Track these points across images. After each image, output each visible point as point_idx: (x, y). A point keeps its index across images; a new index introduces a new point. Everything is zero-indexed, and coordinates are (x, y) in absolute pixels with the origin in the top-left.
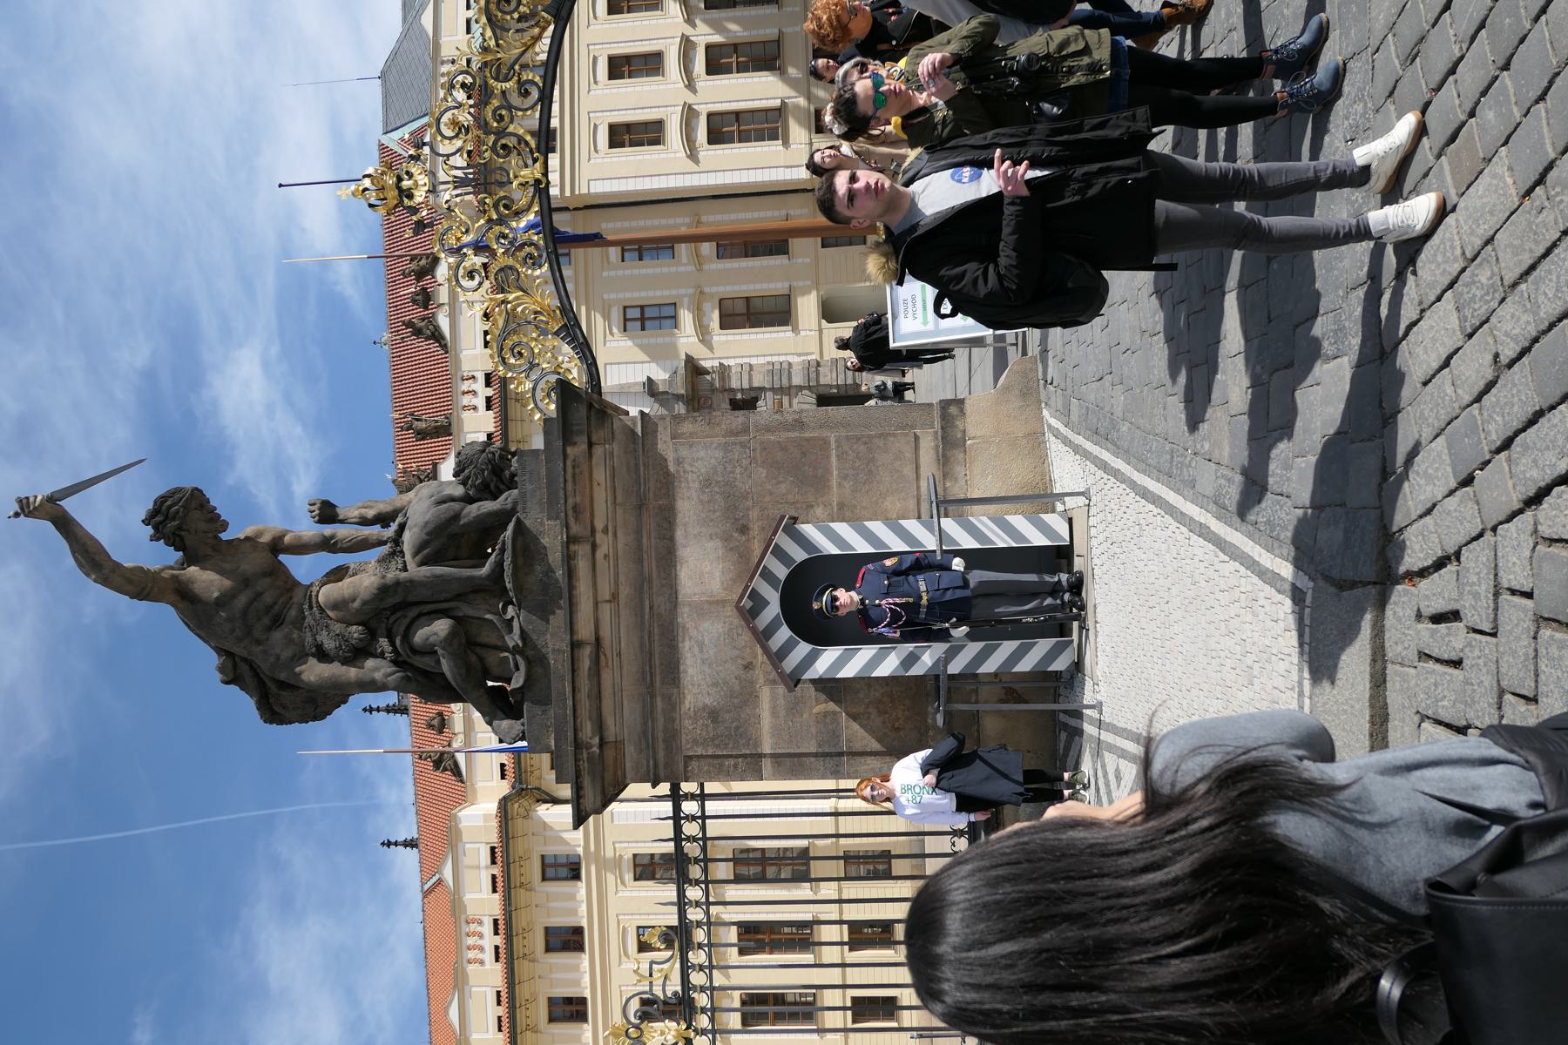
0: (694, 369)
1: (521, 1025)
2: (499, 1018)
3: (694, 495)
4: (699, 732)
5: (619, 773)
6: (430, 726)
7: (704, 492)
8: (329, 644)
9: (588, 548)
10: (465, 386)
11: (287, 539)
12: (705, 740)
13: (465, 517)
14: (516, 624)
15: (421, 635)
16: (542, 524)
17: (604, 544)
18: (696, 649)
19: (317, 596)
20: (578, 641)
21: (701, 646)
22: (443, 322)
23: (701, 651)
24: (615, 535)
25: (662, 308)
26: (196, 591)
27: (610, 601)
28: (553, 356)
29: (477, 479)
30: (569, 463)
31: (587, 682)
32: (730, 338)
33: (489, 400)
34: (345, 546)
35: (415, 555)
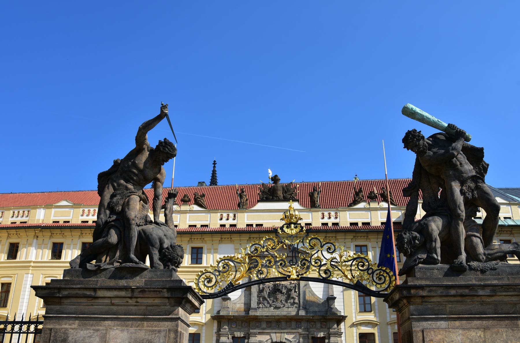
0: (341, 319)
1: (53, 231)
2: (58, 222)
3: (147, 337)
4: (59, 334)
5: (50, 303)
6: (185, 196)
7: (147, 341)
8: (115, 199)
9: (129, 295)
10: (333, 214)
11: (159, 183)
12: (56, 336)
13: (152, 249)
14: (111, 266)
15: (113, 232)
16: (145, 278)
17: (132, 302)
18: (89, 335)
19: (134, 195)
20: (96, 291)
21: (90, 337)
22: (362, 205)
23: (89, 337)
24: (135, 306)
25: (370, 305)
26: (139, 156)
27: (111, 302)
28: (222, 280)
29: (168, 253)
30: (161, 290)
31: (82, 293)
32: (355, 338)
33: (326, 224)
34: (155, 203)
35: (142, 230)
